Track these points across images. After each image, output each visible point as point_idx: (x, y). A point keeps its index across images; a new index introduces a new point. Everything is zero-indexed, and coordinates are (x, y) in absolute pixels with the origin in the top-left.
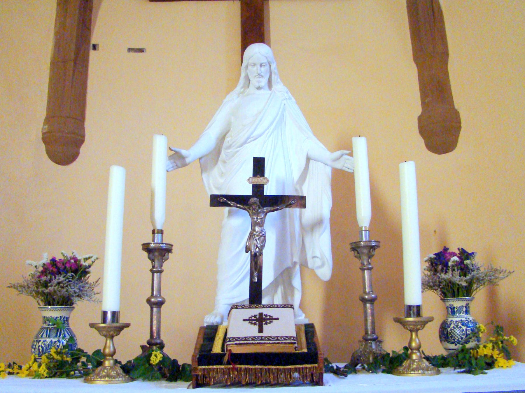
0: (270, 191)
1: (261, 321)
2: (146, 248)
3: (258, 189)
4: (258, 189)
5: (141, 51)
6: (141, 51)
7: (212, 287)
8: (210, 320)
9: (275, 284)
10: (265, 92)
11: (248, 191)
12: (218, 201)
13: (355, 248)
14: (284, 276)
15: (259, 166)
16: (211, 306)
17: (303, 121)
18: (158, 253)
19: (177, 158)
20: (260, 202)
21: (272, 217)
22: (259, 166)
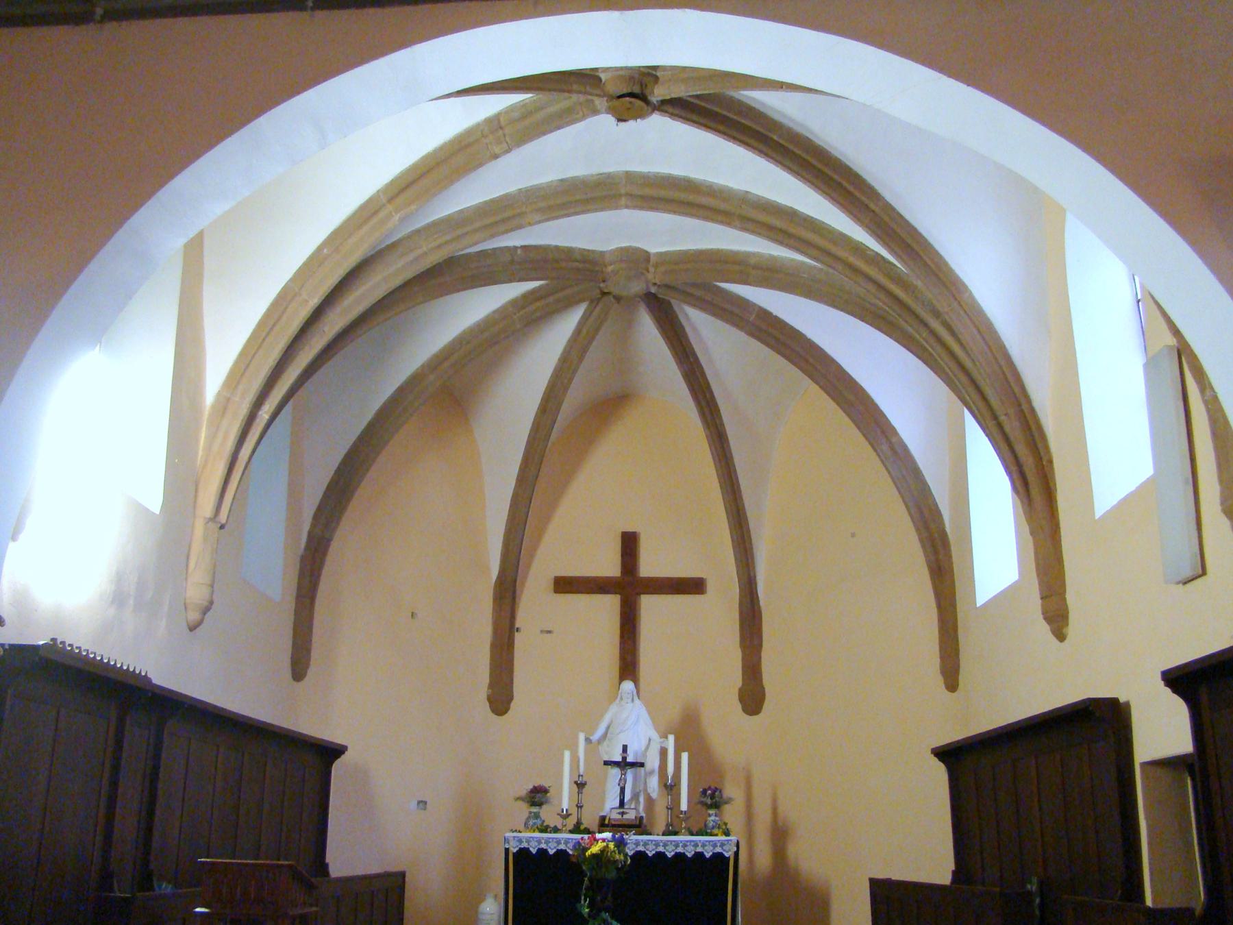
0: (629, 759)
1: (623, 814)
2: (576, 783)
3: (624, 758)
4: (624, 758)
5: (549, 632)
6: (549, 632)
7: (603, 802)
8: (603, 814)
9: (632, 799)
10: (630, 705)
11: (619, 759)
12: (606, 763)
13: (665, 786)
14: (635, 796)
15: (625, 748)
16: (602, 809)
17: (649, 721)
18: (580, 785)
19: (588, 740)
20: (624, 765)
21: (630, 774)
22: (625, 748)
